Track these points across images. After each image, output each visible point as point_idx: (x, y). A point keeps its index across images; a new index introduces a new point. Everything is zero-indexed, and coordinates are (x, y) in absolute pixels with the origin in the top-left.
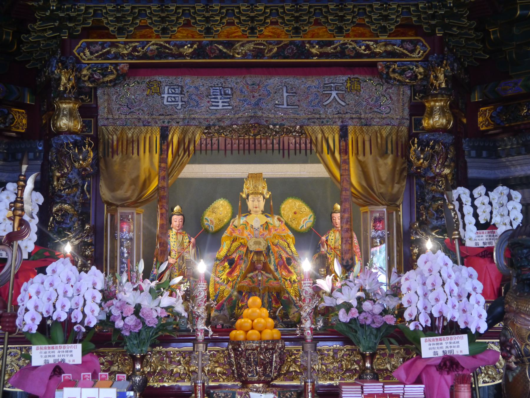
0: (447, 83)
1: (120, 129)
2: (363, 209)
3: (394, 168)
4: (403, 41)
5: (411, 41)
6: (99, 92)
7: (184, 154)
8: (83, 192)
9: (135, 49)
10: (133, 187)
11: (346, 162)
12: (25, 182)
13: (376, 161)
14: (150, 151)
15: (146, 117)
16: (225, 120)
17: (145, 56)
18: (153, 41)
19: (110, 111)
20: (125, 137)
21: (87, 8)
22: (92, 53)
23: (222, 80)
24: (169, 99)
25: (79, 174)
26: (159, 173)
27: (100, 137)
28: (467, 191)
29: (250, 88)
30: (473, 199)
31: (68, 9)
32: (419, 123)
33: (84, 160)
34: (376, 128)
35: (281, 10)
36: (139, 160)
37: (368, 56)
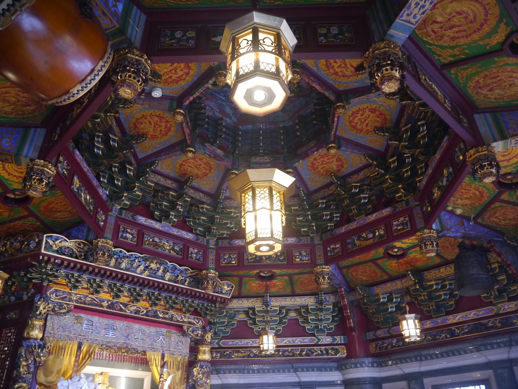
1: (56, 340)
3: (181, 377)
4: (194, 318)
7: (88, 358)
10: (57, 375)
14: (70, 355)
15: (72, 335)
16: (111, 343)
19: (53, 329)
20: (58, 345)
22: (56, 296)
23: (112, 321)
24: (86, 328)
26: (73, 368)
29: (125, 328)
36: (63, 360)
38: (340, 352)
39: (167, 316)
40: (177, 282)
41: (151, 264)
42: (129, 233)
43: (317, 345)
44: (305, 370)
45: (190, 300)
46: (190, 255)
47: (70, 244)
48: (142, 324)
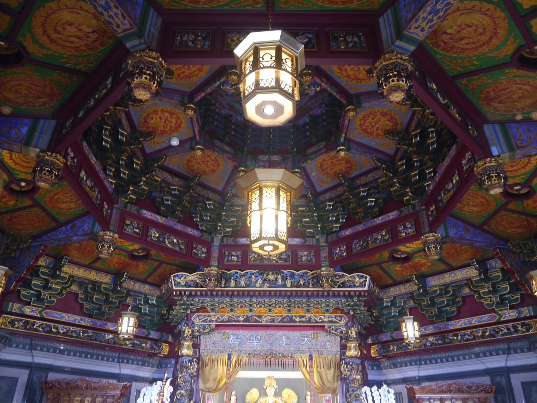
0: (356, 335)
1: (210, 354)
2: (320, 395)
4: (336, 316)
5: (339, 316)
6: (202, 337)
8: (191, 384)
9: (218, 318)
11: (312, 372)
12: (166, 382)
13: (326, 371)
17: (223, 321)
18: (227, 314)
19: (206, 346)
21: (199, 300)
22: (199, 320)
25: (190, 375)
27: (201, 358)
28: (369, 389)
30: (372, 393)
31: (191, 301)
32: (344, 353)
33: (193, 369)
34: (325, 355)
35: (282, 302)
36: (217, 369)
37: (321, 322)
38: (532, 327)
39: (304, 319)
40: (300, 286)
41: (269, 276)
42: (234, 256)
43: (499, 322)
44: (494, 353)
45: (324, 300)
46: (299, 260)
47: (192, 277)
48: (285, 330)
